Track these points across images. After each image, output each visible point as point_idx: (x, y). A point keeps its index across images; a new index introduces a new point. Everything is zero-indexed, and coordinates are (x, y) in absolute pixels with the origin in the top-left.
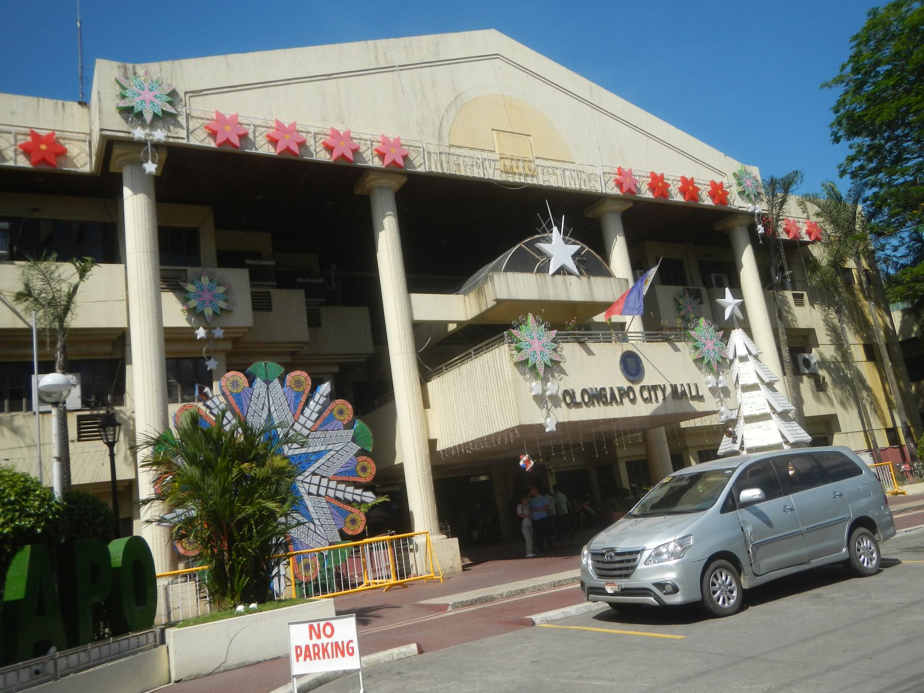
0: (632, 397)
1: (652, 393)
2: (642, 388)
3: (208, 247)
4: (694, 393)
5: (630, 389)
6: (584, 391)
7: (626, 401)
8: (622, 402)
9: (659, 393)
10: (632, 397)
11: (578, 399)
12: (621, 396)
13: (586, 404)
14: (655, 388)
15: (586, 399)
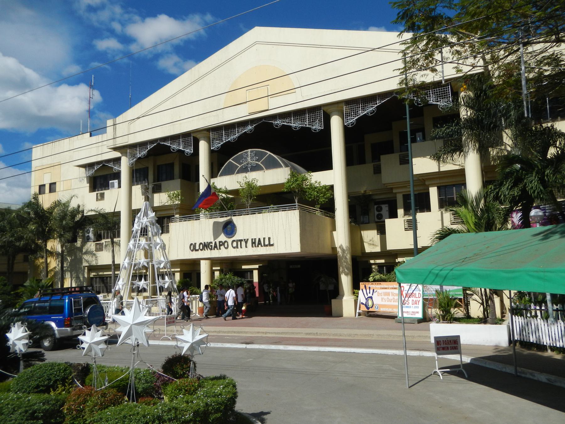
0: (226, 246)
1: (239, 243)
2: (234, 241)
3: (177, 170)
4: (267, 243)
5: (226, 241)
6: (201, 243)
7: (222, 247)
8: (220, 249)
9: (243, 243)
10: (226, 246)
11: (197, 248)
12: (220, 245)
13: (201, 250)
14: (241, 241)
15: (201, 248)
